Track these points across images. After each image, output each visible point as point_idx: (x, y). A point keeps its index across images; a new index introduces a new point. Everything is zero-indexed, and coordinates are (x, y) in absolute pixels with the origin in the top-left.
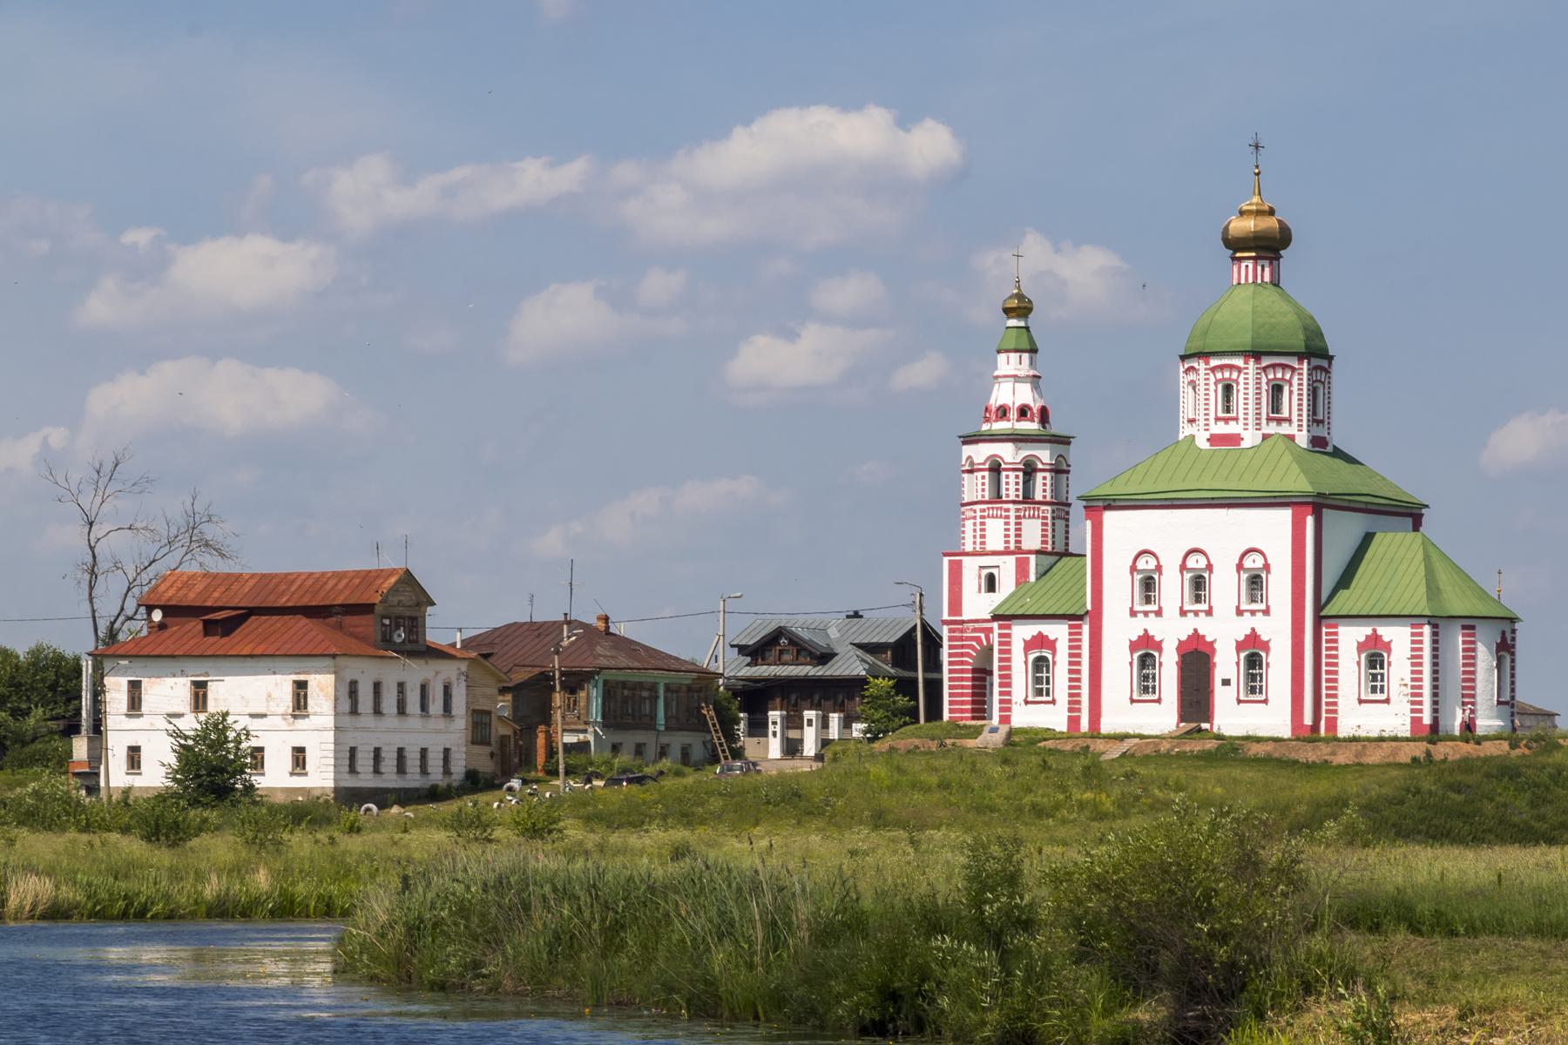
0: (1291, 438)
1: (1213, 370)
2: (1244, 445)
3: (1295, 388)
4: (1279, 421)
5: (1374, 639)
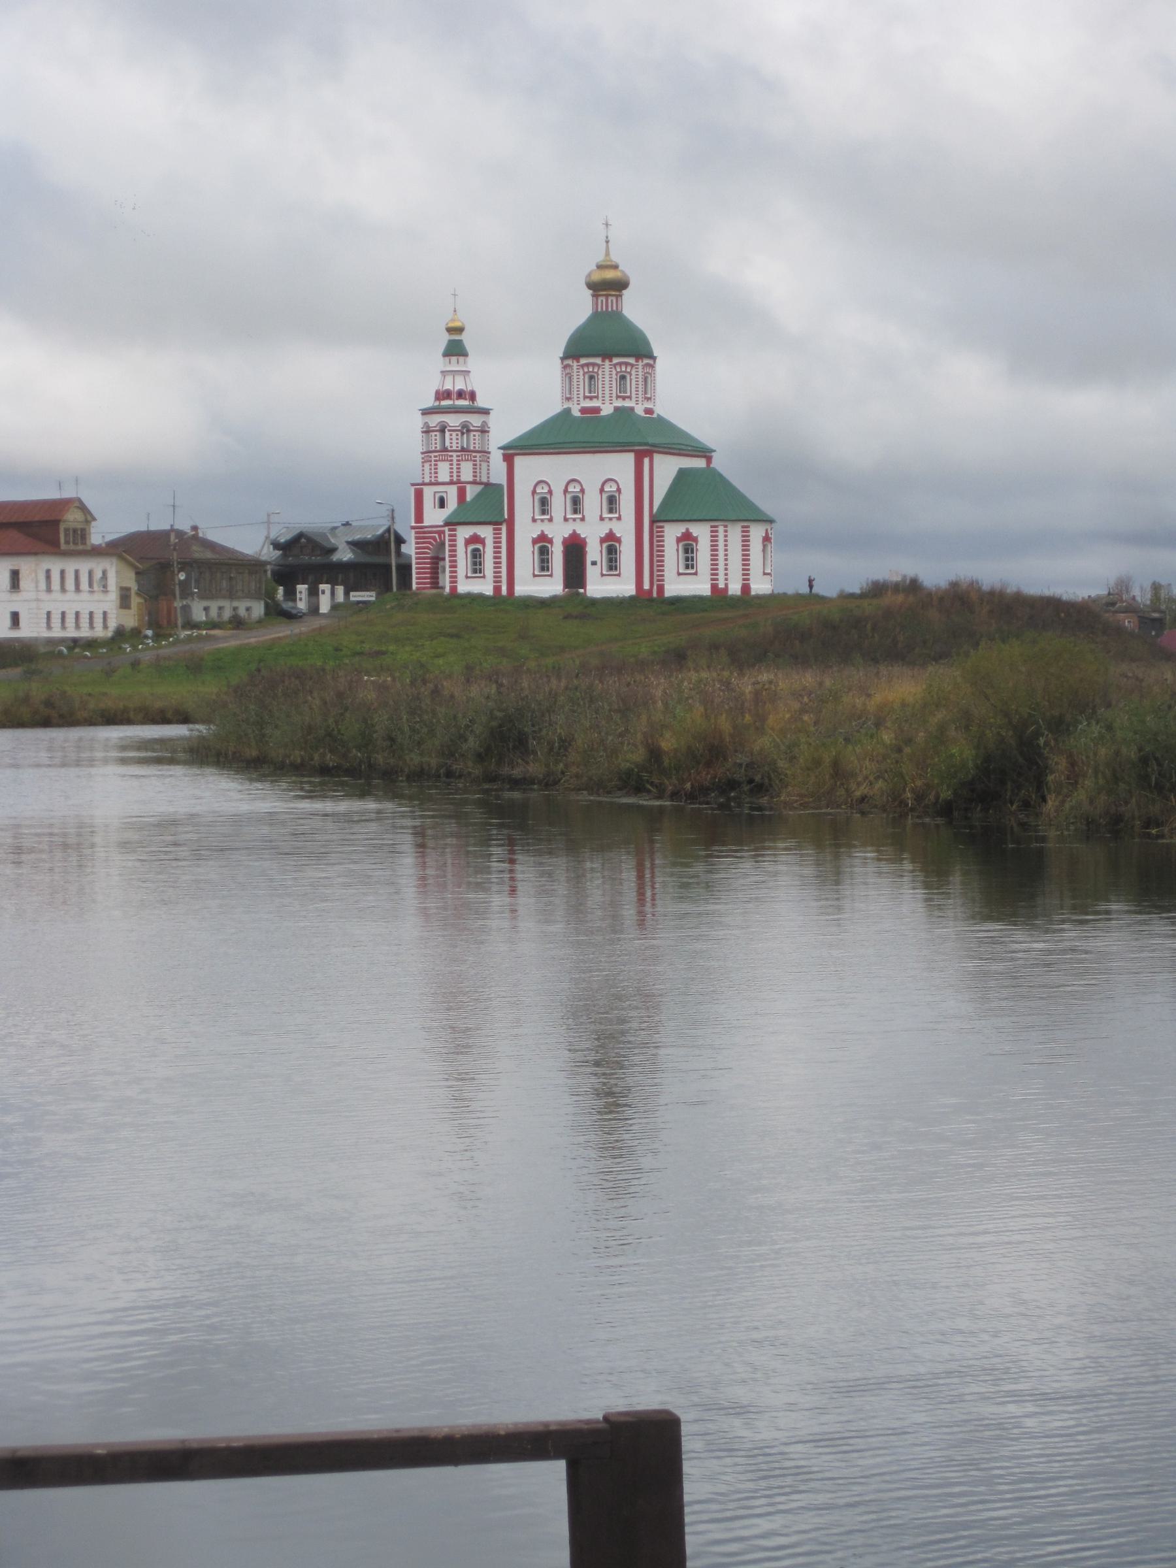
0: (632, 409)
1: (583, 366)
2: (603, 413)
3: (633, 377)
4: (624, 398)
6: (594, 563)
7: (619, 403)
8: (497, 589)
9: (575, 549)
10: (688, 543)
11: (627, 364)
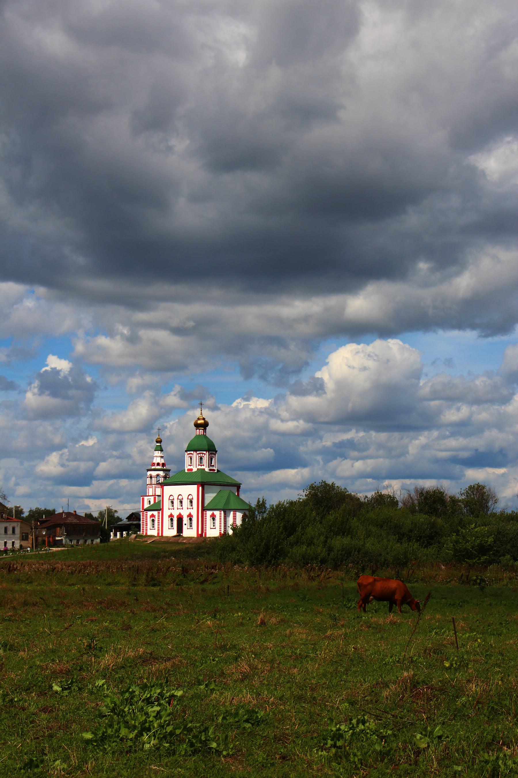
5: (213, 514)
6: (185, 524)
7: (200, 467)
8: (158, 533)
9: (180, 519)
10: (213, 517)
11: (202, 453)
